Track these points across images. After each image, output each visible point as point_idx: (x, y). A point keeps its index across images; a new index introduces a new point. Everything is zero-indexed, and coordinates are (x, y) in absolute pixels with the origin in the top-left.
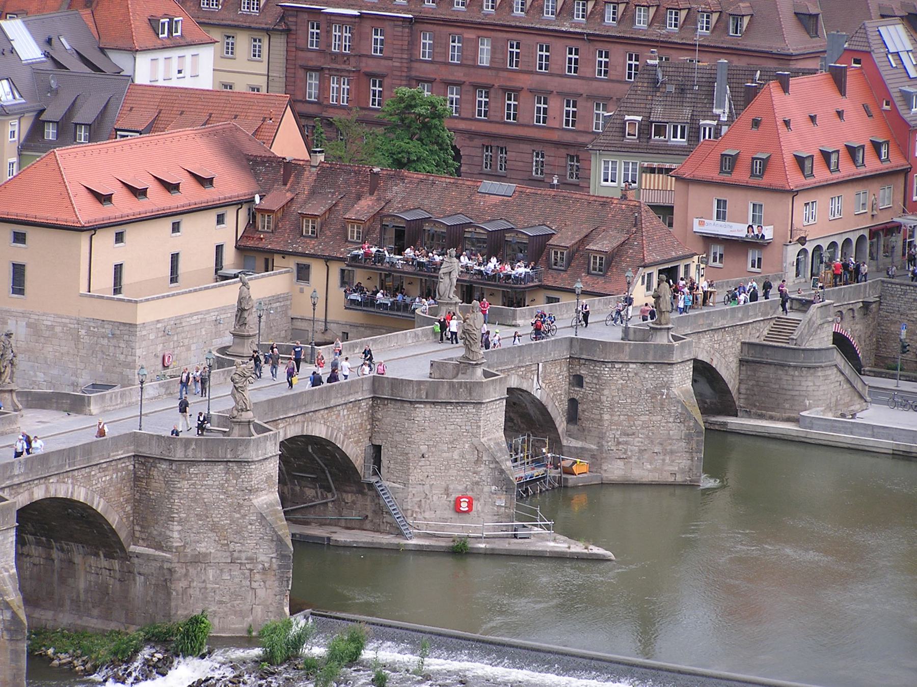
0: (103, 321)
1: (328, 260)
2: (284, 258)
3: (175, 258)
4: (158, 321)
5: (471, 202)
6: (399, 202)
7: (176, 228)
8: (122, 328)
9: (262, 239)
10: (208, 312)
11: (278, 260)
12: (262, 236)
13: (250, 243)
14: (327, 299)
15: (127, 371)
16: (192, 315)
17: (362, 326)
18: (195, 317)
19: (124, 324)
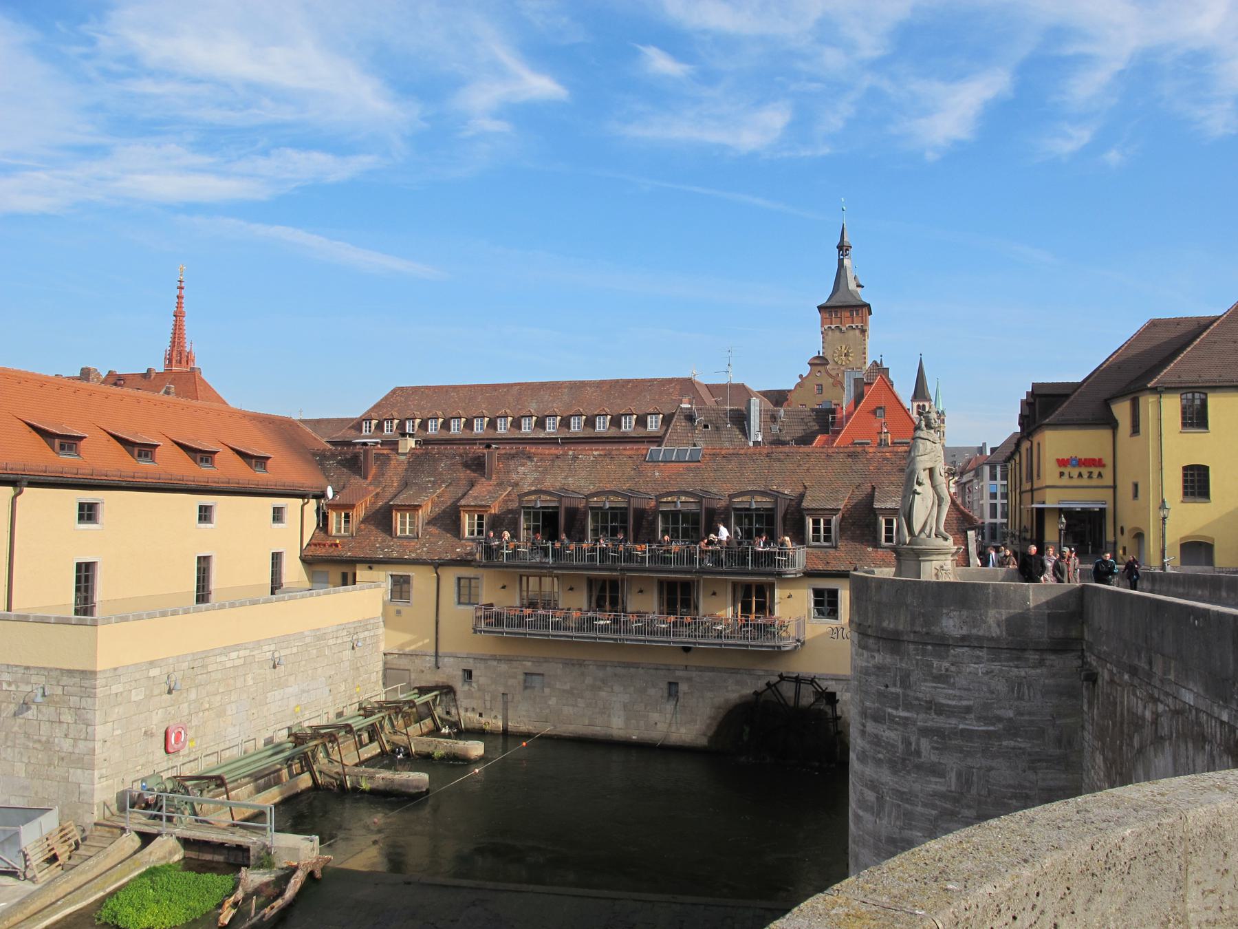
0: (27, 668)
1: (438, 565)
2: (370, 568)
3: (204, 564)
4: (152, 664)
5: (640, 474)
6: (531, 485)
7: (205, 514)
8: (65, 680)
9: (336, 545)
10: (258, 644)
11: (362, 573)
12: (338, 542)
13: (321, 552)
14: (437, 623)
15: (77, 775)
16: (227, 650)
17: (494, 658)
18: (234, 655)
19: (70, 672)
